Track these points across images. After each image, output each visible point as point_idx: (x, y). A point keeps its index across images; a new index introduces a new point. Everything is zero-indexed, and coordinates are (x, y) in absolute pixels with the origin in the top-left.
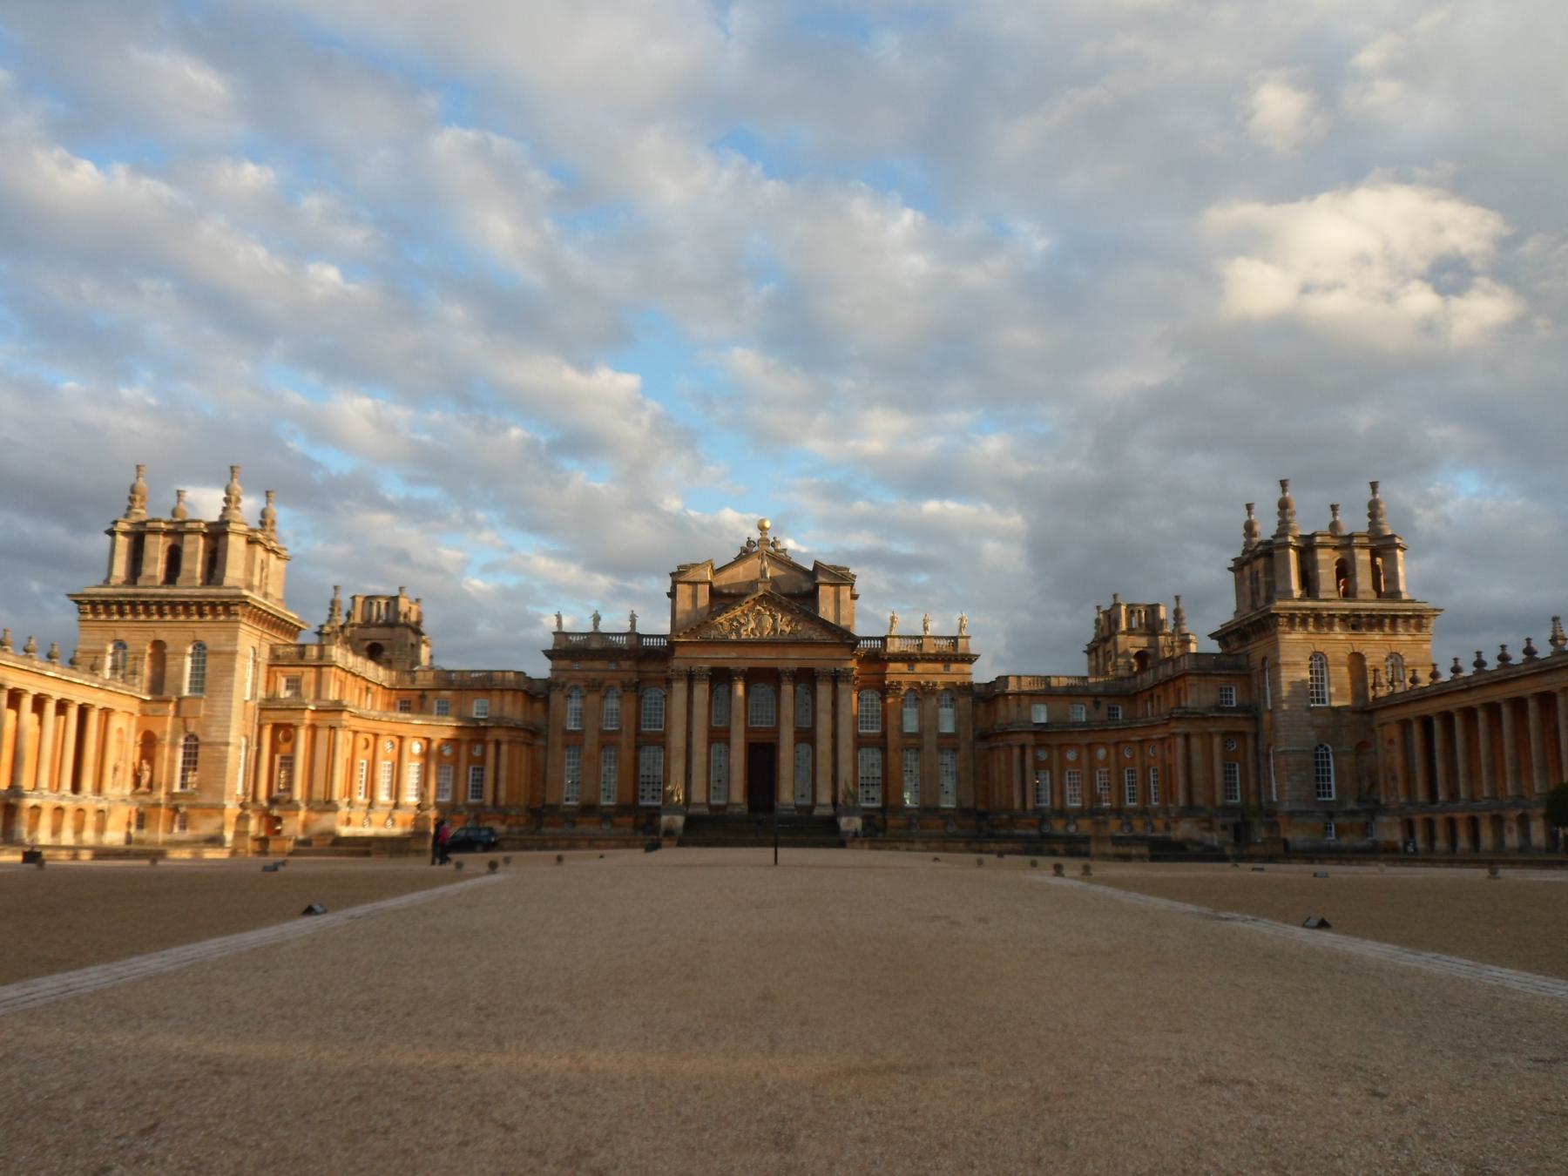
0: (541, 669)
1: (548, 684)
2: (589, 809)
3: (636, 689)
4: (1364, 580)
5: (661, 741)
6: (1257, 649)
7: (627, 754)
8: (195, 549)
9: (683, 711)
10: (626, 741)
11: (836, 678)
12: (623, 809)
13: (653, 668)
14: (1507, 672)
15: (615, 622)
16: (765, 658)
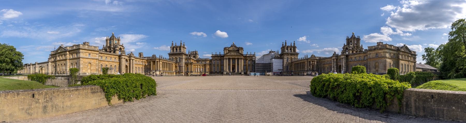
0: (211, 58)
1: (212, 60)
2: (216, 72)
3: (220, 60)
4: (292, 51)
5: (223, 65)
6: (282, 56)
7: (220, 67)
8: (178, 49)
9: (226, 62)
10: (220, 65)
11: (241, 59)
12: (219, 72)
13: (222, 58)
14: (302, 60)
15: (218, 53)
16: (234, 57)
